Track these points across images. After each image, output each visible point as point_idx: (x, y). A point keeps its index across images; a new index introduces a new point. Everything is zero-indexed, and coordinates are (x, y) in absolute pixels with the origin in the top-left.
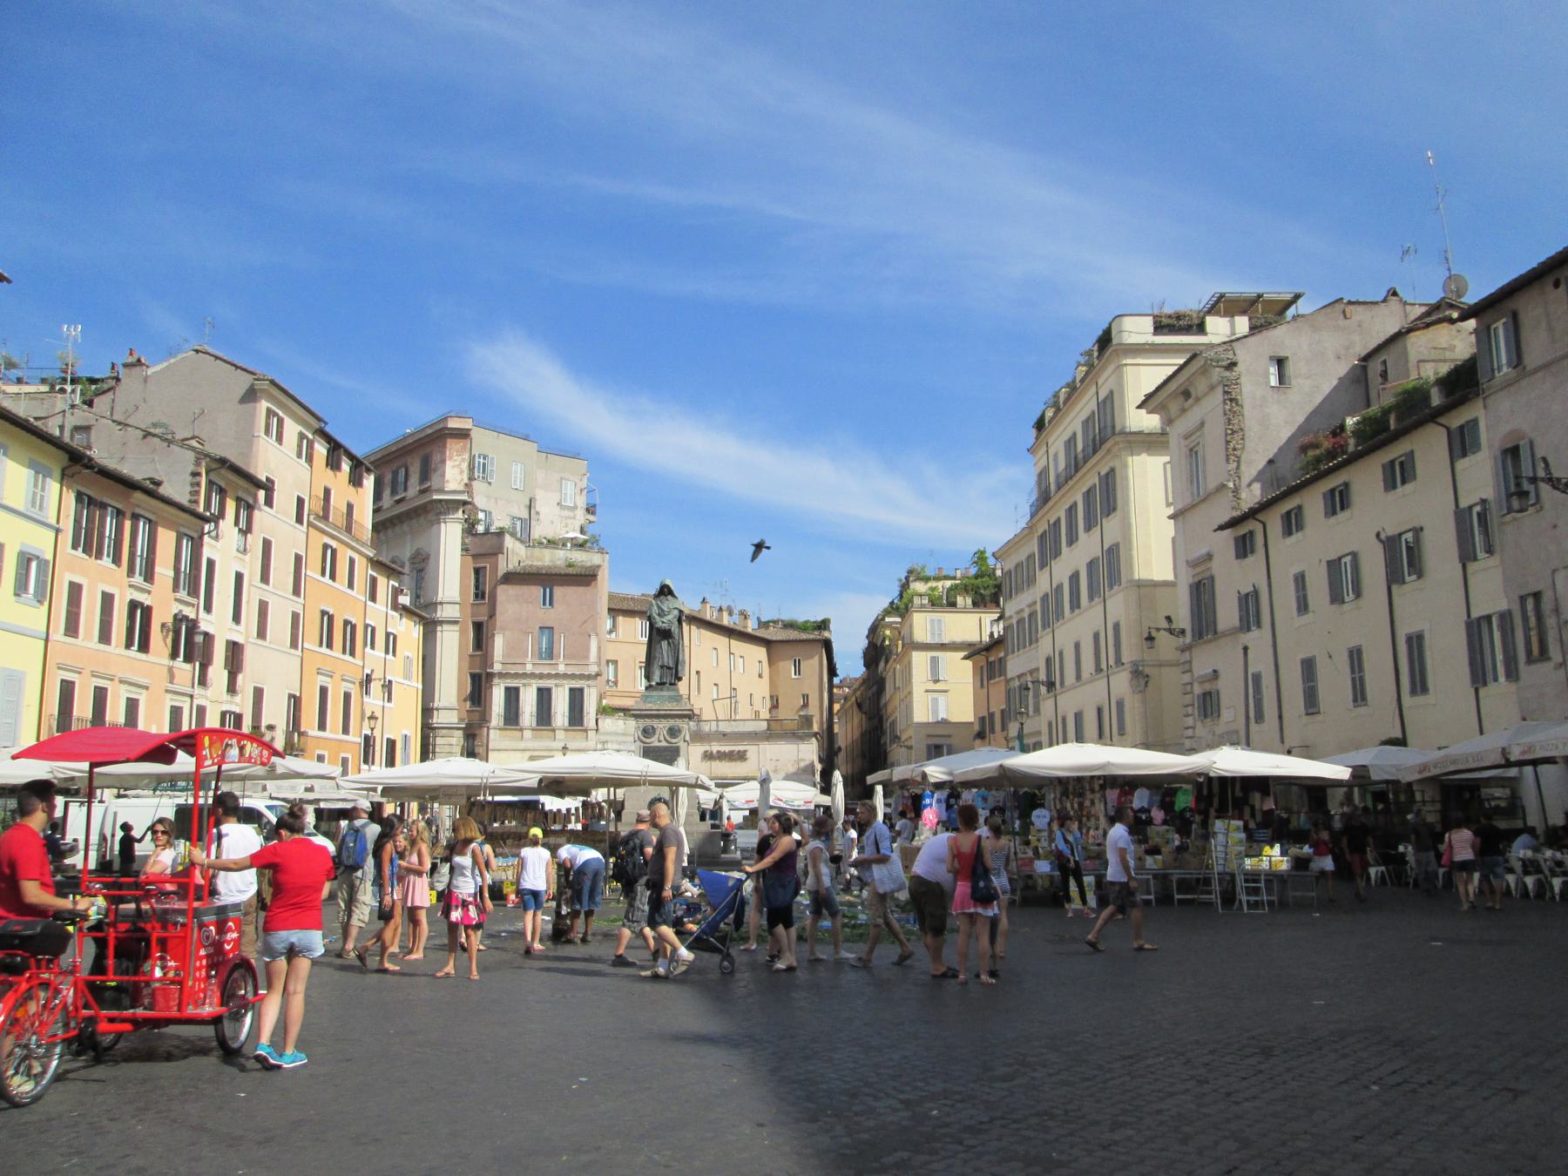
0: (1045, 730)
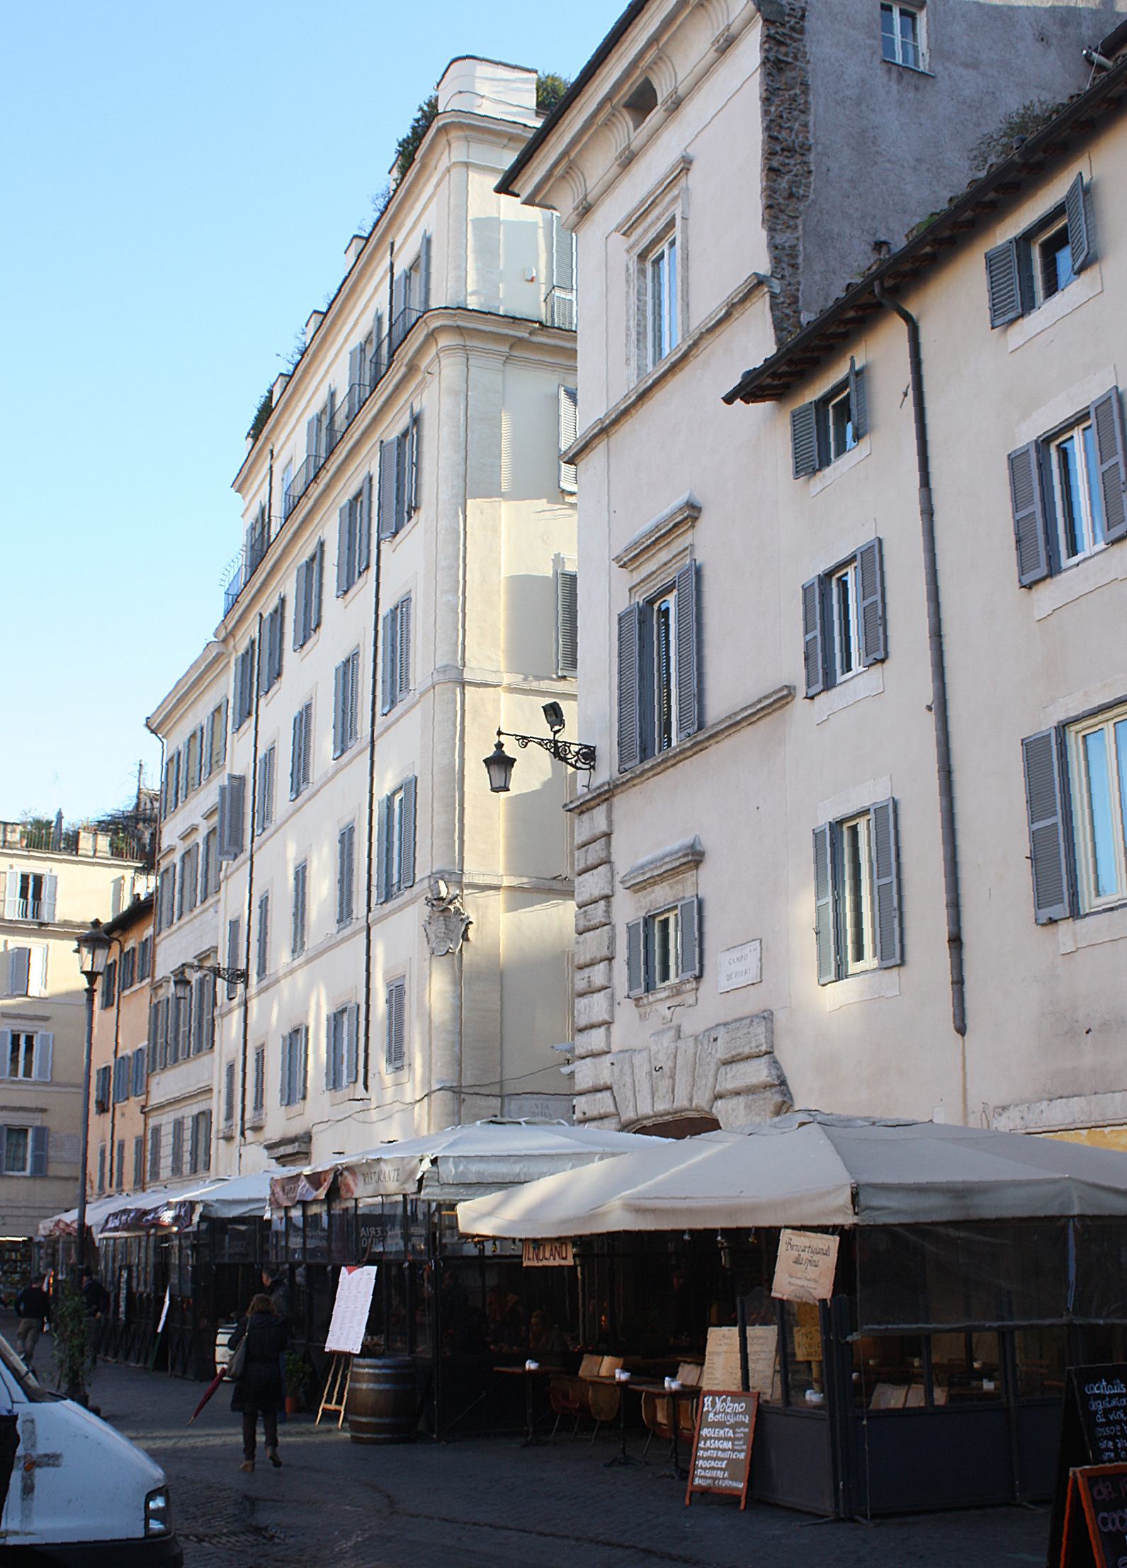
0: (220, 1084)
